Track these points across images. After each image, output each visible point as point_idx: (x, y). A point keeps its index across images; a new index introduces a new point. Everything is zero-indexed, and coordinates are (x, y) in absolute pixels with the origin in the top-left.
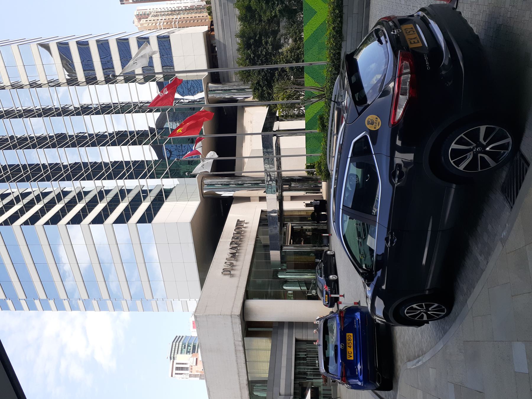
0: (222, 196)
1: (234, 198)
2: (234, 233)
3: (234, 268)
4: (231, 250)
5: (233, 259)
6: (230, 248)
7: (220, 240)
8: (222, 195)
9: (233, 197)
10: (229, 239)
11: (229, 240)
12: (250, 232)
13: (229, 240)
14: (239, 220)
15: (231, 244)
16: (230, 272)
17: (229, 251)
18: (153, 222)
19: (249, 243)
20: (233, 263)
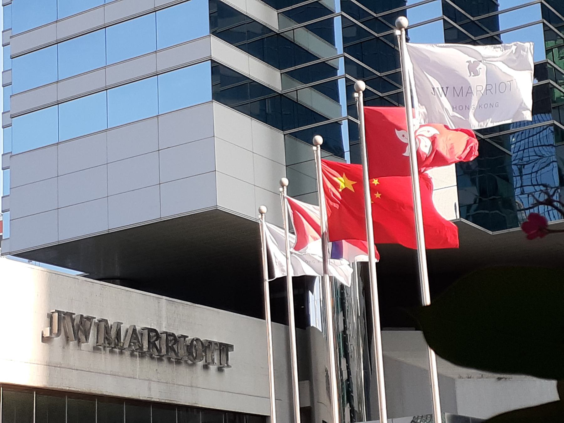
0: (310, 292)
1: (305, 329)
2: (185, 337)
3: (72, 344)
4: (130, 332)
5: (101, 340)
6: (134, 330)
7: (164, 297)
8: (312, 292)
9: (307, 328)
10: (169, 325)
11: (164, 324)
12: (192, 386)
13: (164, 324)
14: (233, 351)
15: (151, 330)
16: (58, 335)
17: (128, 326)
18: (219, 108)
19: (154, 385)
20: (87, 338)
